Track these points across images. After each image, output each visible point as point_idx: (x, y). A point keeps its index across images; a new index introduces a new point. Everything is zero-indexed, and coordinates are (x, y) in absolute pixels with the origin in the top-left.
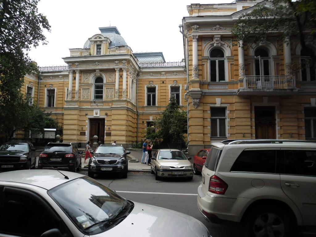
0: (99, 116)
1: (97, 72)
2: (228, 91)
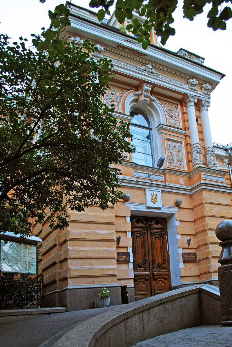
0: (160, 206)
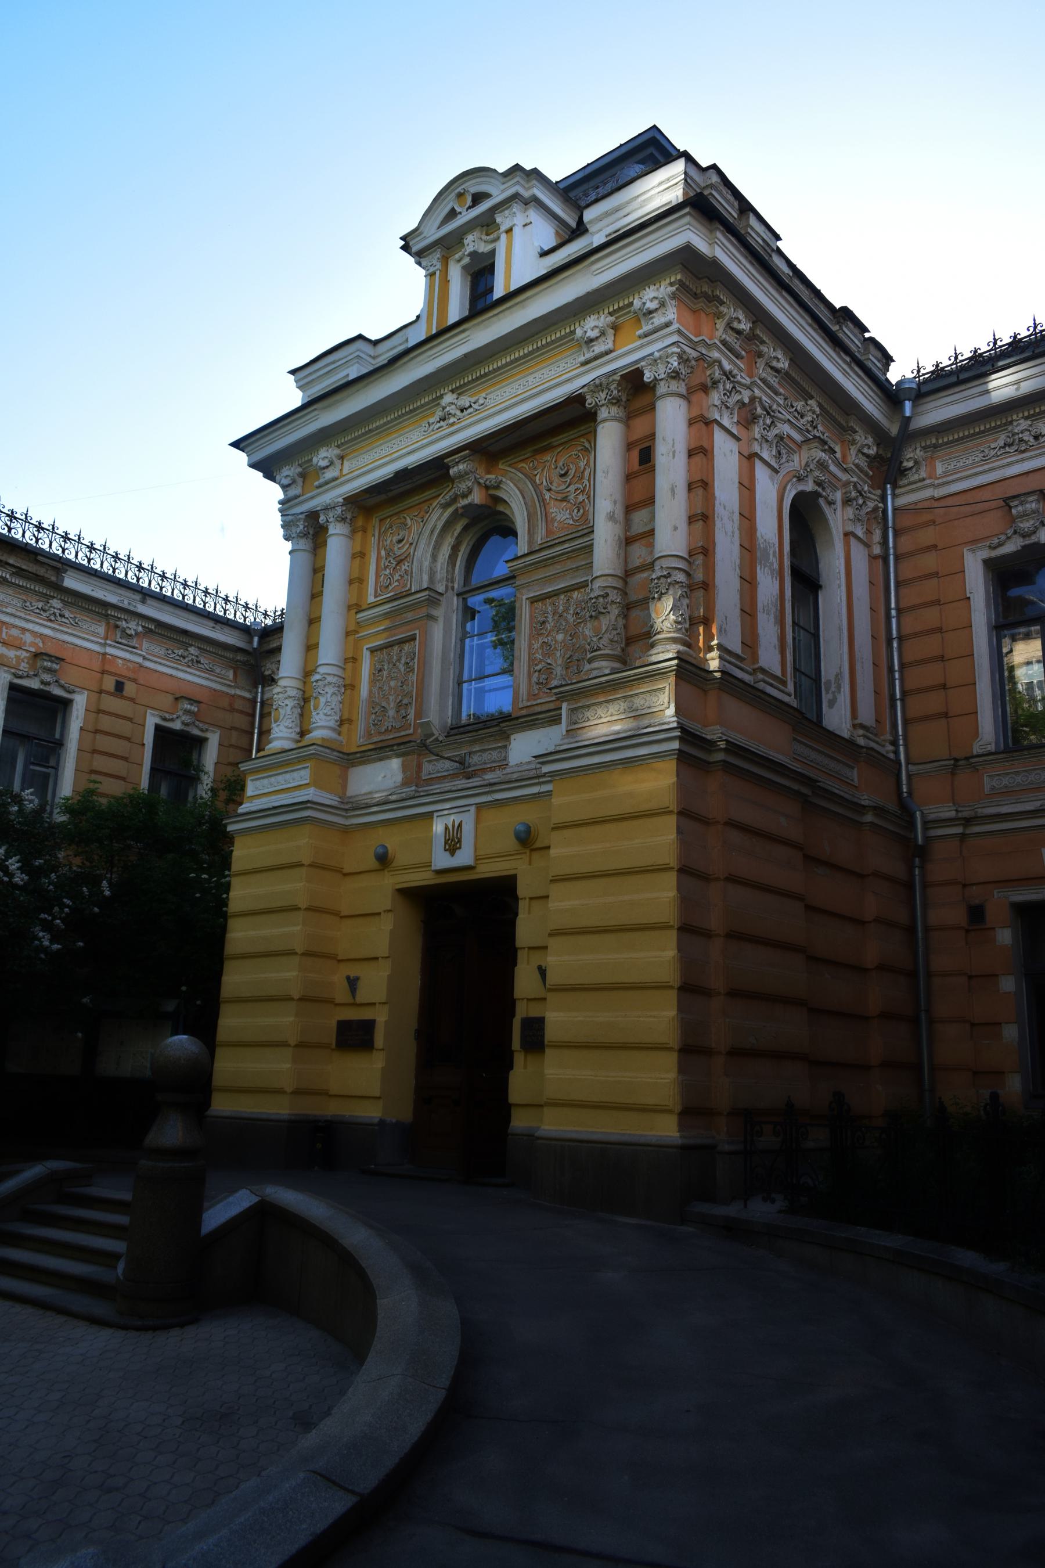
1: (462, 476)
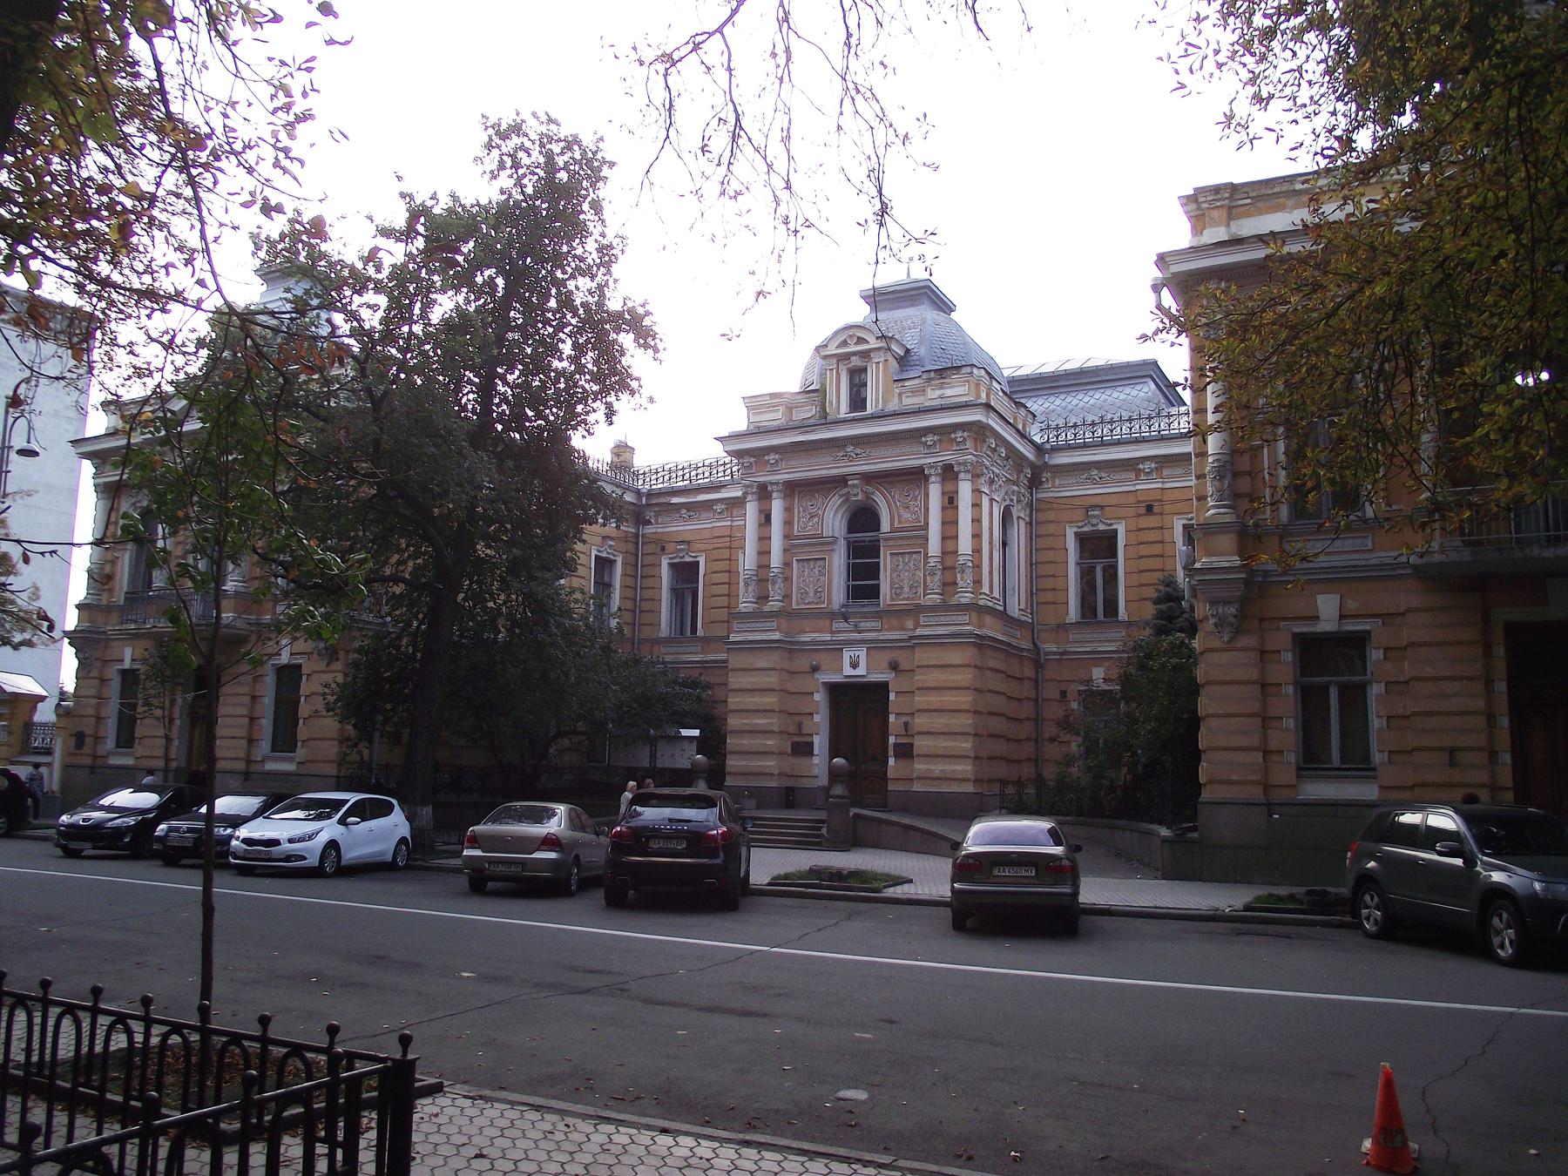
2: (1375, 558)
